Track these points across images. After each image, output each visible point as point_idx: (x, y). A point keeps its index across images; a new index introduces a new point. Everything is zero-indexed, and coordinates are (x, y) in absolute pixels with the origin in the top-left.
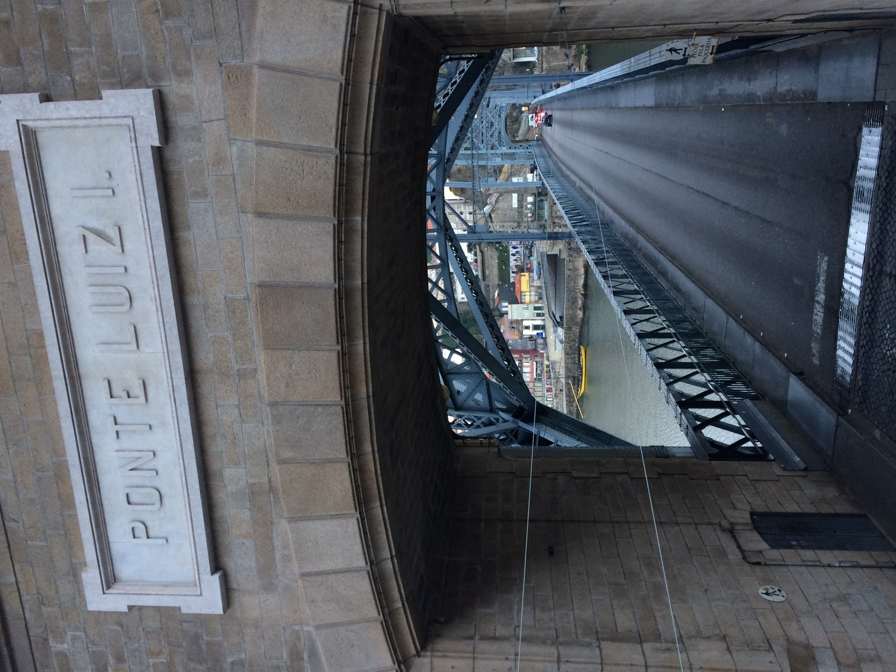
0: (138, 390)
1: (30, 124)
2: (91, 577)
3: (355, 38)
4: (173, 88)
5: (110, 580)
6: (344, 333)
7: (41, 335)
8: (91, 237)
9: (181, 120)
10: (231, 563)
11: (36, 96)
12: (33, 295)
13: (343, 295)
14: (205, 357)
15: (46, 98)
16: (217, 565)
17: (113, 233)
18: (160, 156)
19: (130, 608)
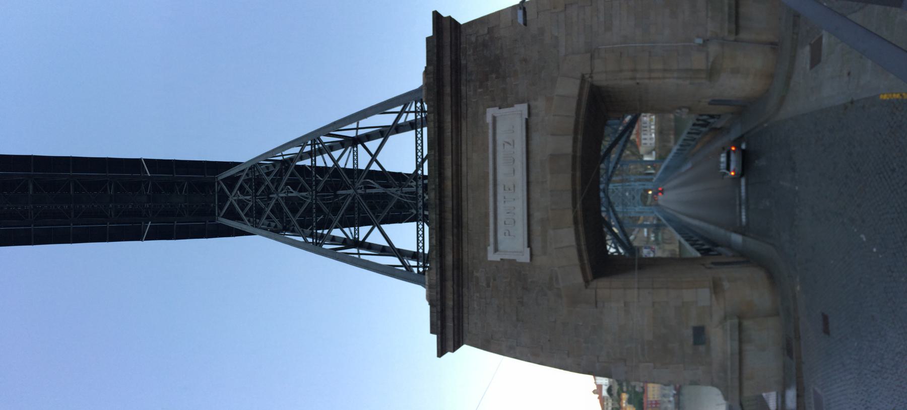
0: (512, 188)
1: (495, 115)
2: (491, 249)
3: (581, 89)
4: (533, 103)
5: (496, 250)
6: (574, 169)
7: (488, 173)
8: (506, 144)
9: (533, 111)
10: (533, 246)
11: (498, 108)
12: (488, 162)
13: (574, 157)
14: (532, 178)
15: (500, 108)
16: (529, 246)
17: (511, 142)
18: (527, 121)
19: (502, 259)
